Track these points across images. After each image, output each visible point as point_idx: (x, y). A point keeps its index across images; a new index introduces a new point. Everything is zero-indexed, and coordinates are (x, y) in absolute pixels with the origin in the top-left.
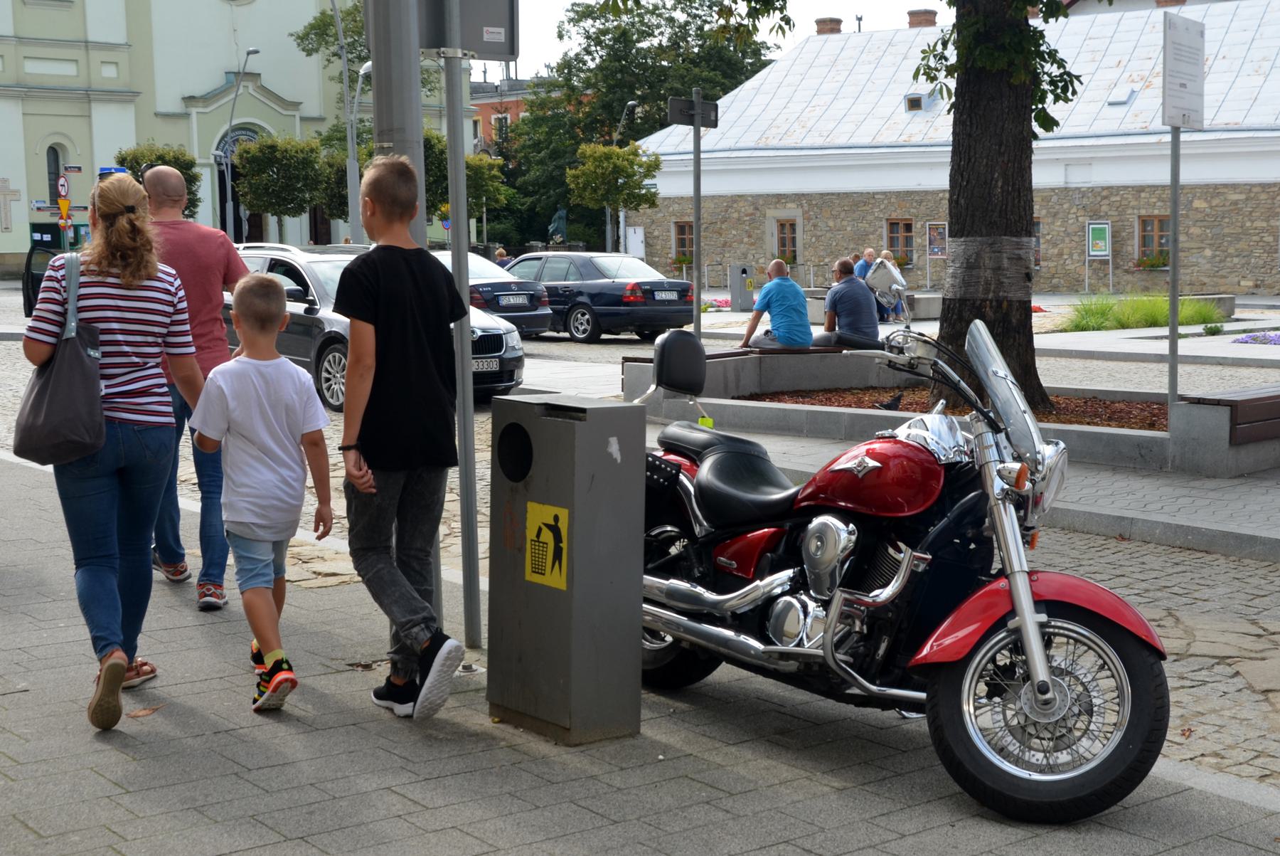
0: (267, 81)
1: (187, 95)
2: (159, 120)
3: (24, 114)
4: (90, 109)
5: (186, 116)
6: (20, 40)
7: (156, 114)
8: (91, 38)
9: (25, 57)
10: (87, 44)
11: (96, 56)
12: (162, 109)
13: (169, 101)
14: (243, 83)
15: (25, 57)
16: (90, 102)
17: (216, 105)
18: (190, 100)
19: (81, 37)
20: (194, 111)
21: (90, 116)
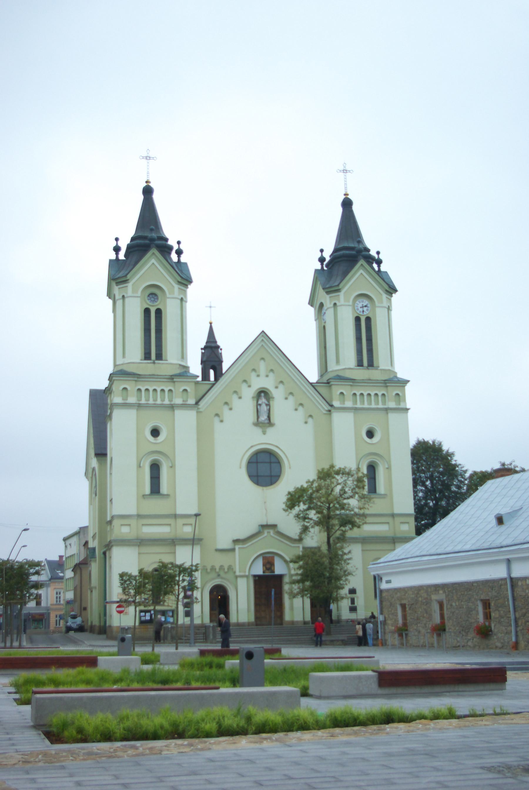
0: (282, 528)
1: (235, 538)
2: (218, 554)
3: (139, 554)
4: (175, 550)
5: (233, 550)
6: (139, 516)
7: (217, 550)
8: (179, 512)
9: (143, 525)
10: (175, 516)
11: (180, 521)
12: (220, 547)
13: (224, 543)
14: (266, 531)
15: (143, 525)
16: (175, 545)
17: (250, 543)
18: (236, 541)
19: (173, 513)
20: (237, 547)
21: (175, 553)
